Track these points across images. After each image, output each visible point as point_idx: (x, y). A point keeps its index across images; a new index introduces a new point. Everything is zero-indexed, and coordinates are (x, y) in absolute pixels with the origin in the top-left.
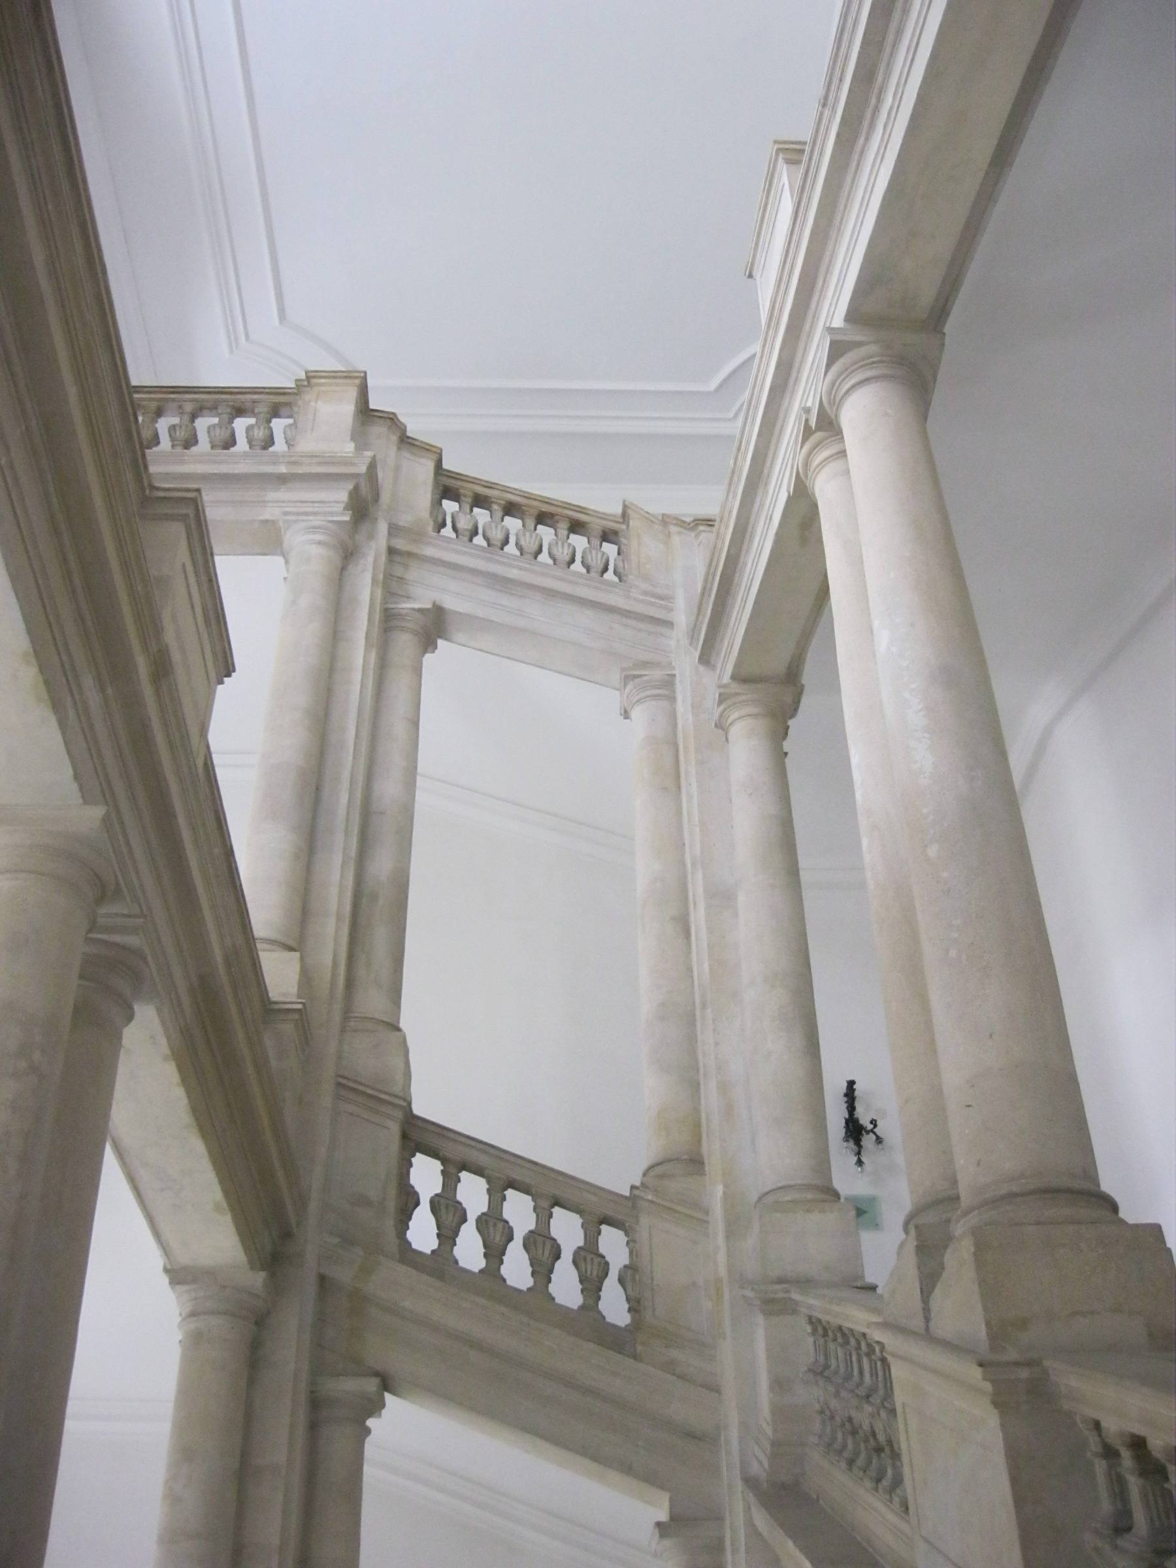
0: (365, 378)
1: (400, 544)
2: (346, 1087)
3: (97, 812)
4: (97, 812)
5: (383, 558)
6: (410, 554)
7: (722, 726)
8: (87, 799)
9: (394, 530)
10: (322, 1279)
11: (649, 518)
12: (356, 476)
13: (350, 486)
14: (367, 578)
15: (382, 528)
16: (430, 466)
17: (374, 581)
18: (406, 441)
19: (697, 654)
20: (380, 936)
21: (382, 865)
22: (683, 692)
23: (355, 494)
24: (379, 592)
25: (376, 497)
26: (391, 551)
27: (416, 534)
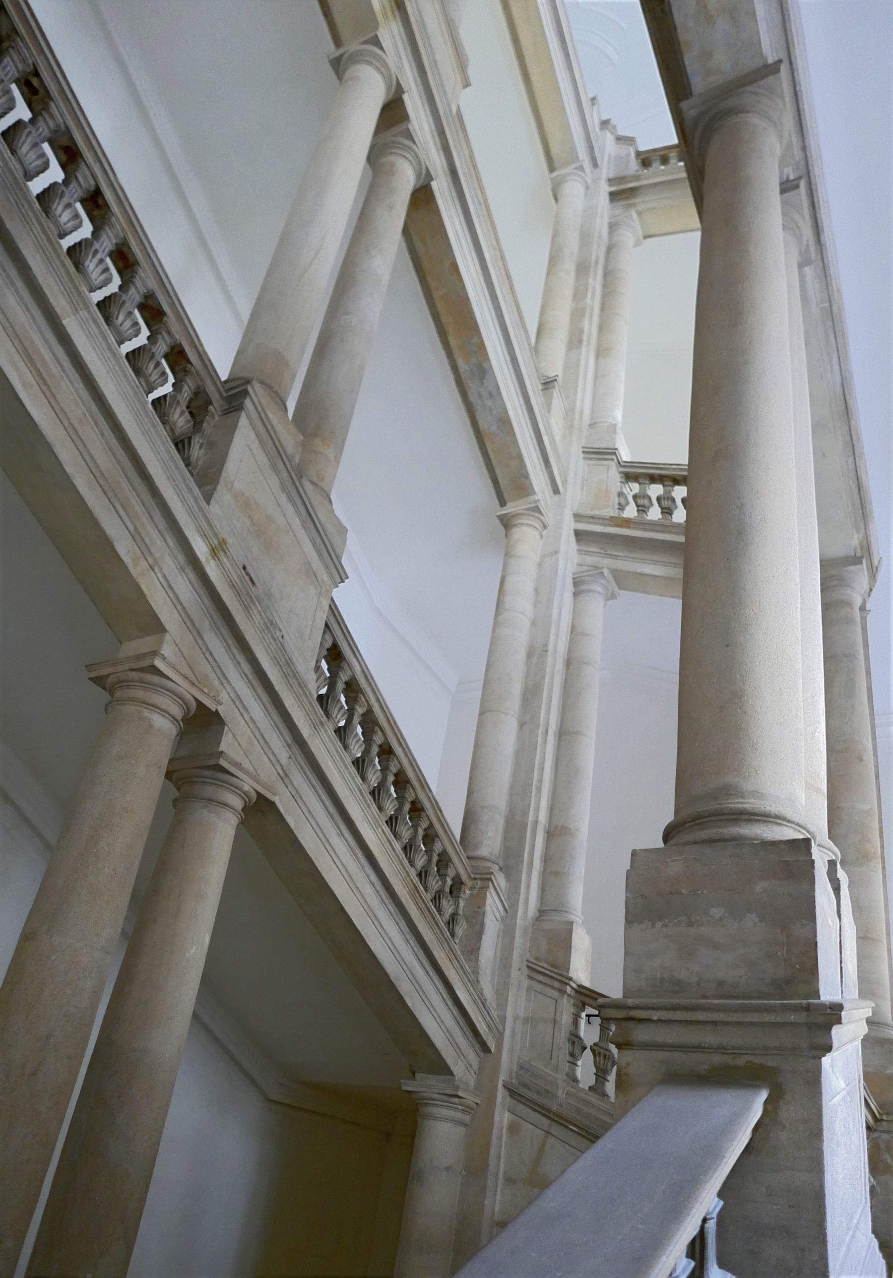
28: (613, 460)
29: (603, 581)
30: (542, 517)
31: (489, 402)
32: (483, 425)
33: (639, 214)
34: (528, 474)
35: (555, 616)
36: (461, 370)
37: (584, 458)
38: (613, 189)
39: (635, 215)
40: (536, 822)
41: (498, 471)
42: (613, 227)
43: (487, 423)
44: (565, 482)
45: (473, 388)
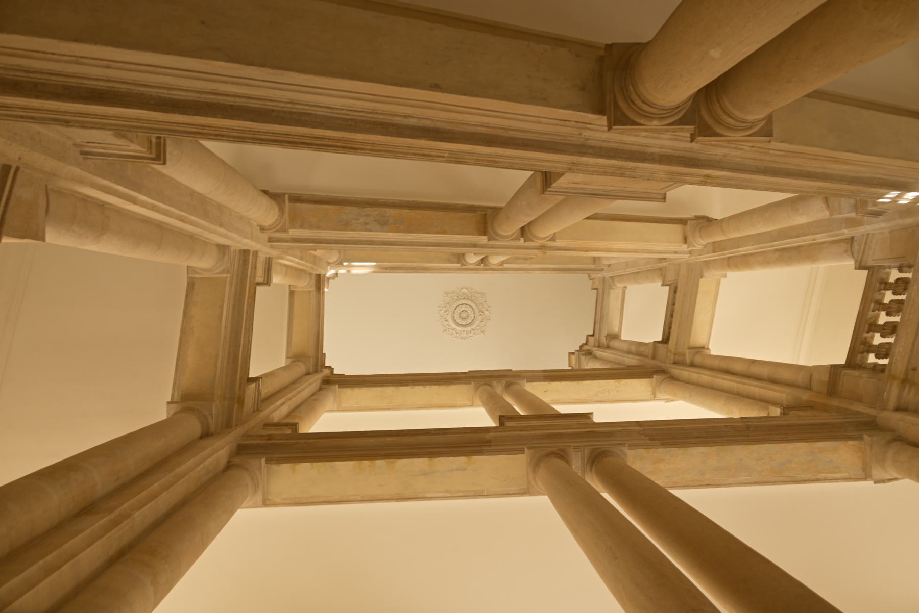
0: (569, 353)
1: (597, 345)
2: (654, 357)
3: (472, 382)
4: (472, 382)
5: (598, 349)
6: (599, 342)
7: (609, 266)
8: (470, 383)
9: (595, 346)
10: (675, 363)
11: (593, 283)
12: (579, 355)
13: (581, 356)
14: (599, 352)
15: (595, 349)
16: (590, 337)
17: (599, 351)
18: (586, 344)
19: (602, 272)
20: (642, 349)
21: (633, 348)
22: (610, 274)
23: (583, 355)
24: (601, 350)
25: (589, 350)
26: (599, 347)
27: (595, 339)
28: (264, 281)
29: (218, 271)
30: (274, 230)
31: (362, 220)
32: (348, 209)
33: (310, 292)
34: (304, 229)
35: (231, 234)
36: (388, 210)
37: (266, 258)
38: (322, 276)
39: (310, 289)
40: (134, 201)
41: (312, 206)
42: (311, 274)
43: (349, 212)
44: (272, 247)
45: (374, 212)
